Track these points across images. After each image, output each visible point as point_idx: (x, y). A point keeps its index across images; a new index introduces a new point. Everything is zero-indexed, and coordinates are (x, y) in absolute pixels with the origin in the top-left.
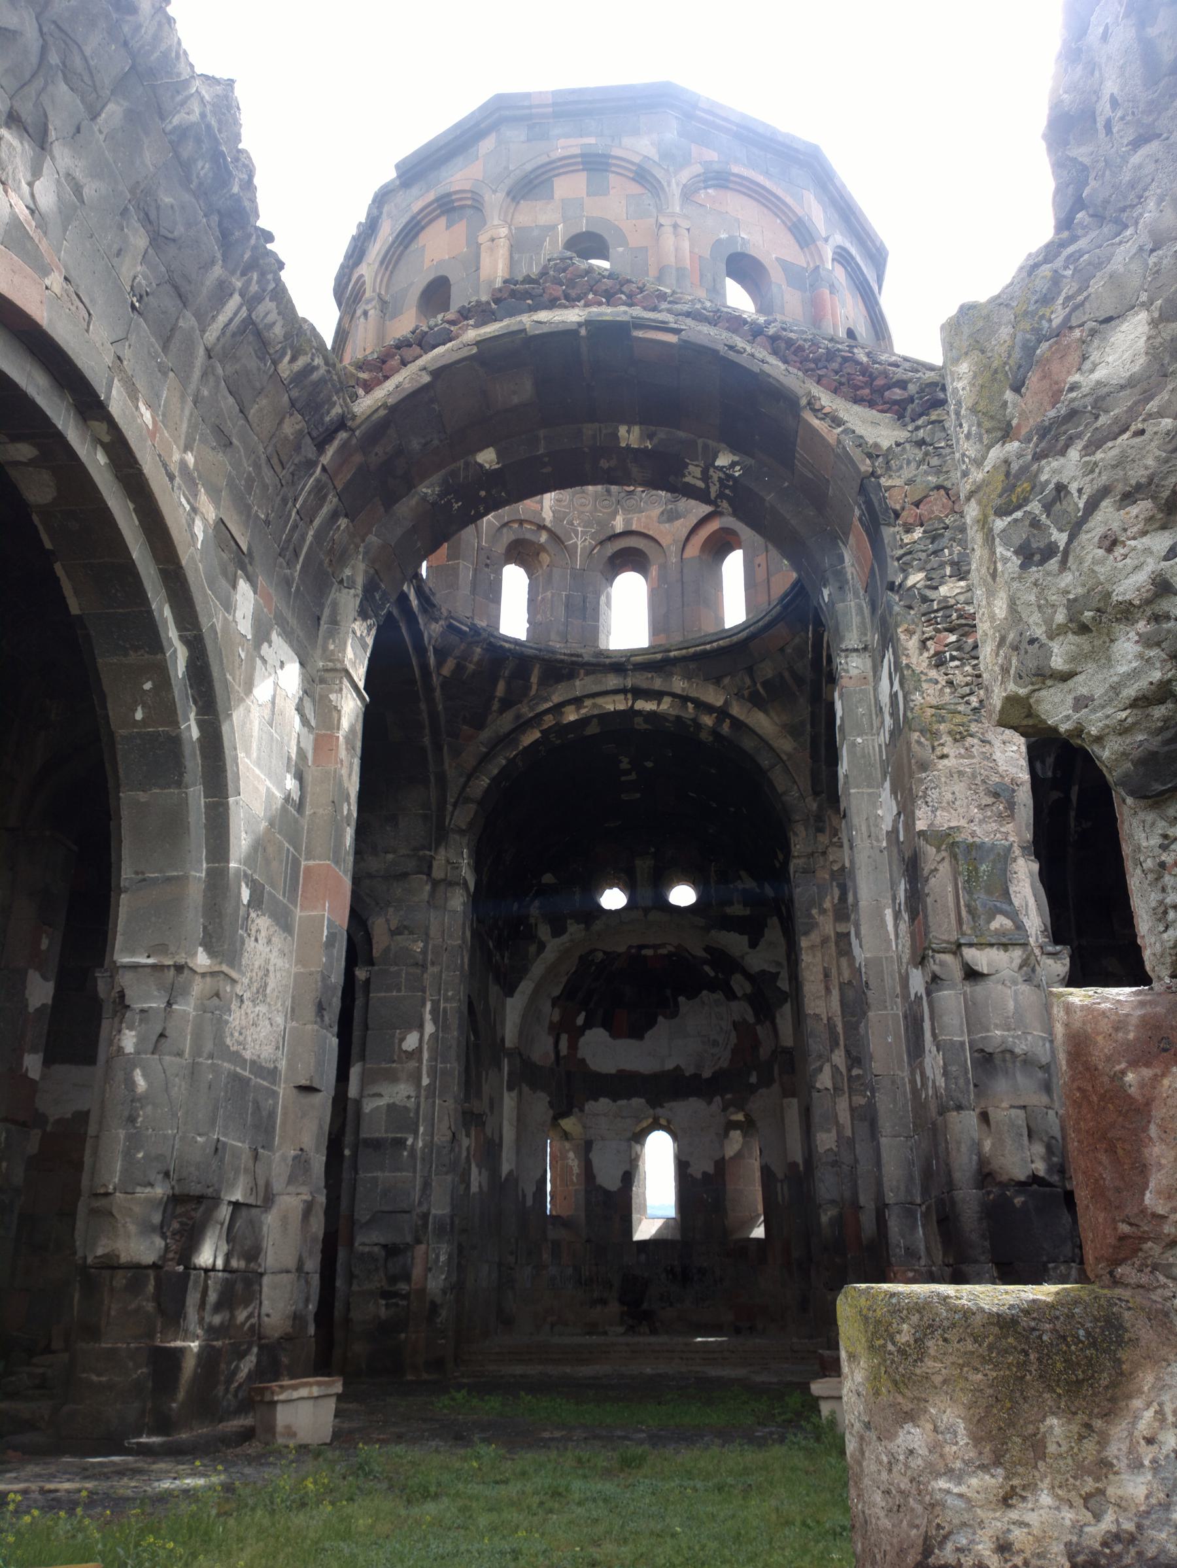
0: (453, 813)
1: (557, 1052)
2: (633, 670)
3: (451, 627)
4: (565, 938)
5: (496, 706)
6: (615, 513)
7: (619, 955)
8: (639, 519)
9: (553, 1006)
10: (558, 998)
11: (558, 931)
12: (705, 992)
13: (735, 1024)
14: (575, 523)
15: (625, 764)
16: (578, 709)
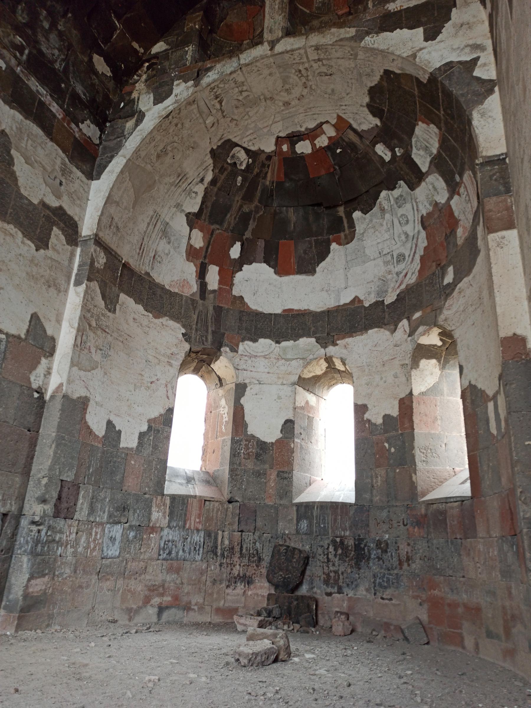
1: (203, 286)
4: (169, 103)
7: (269, 157)
10: (198, 215)
12: (384, 194)
13: (424, 222)
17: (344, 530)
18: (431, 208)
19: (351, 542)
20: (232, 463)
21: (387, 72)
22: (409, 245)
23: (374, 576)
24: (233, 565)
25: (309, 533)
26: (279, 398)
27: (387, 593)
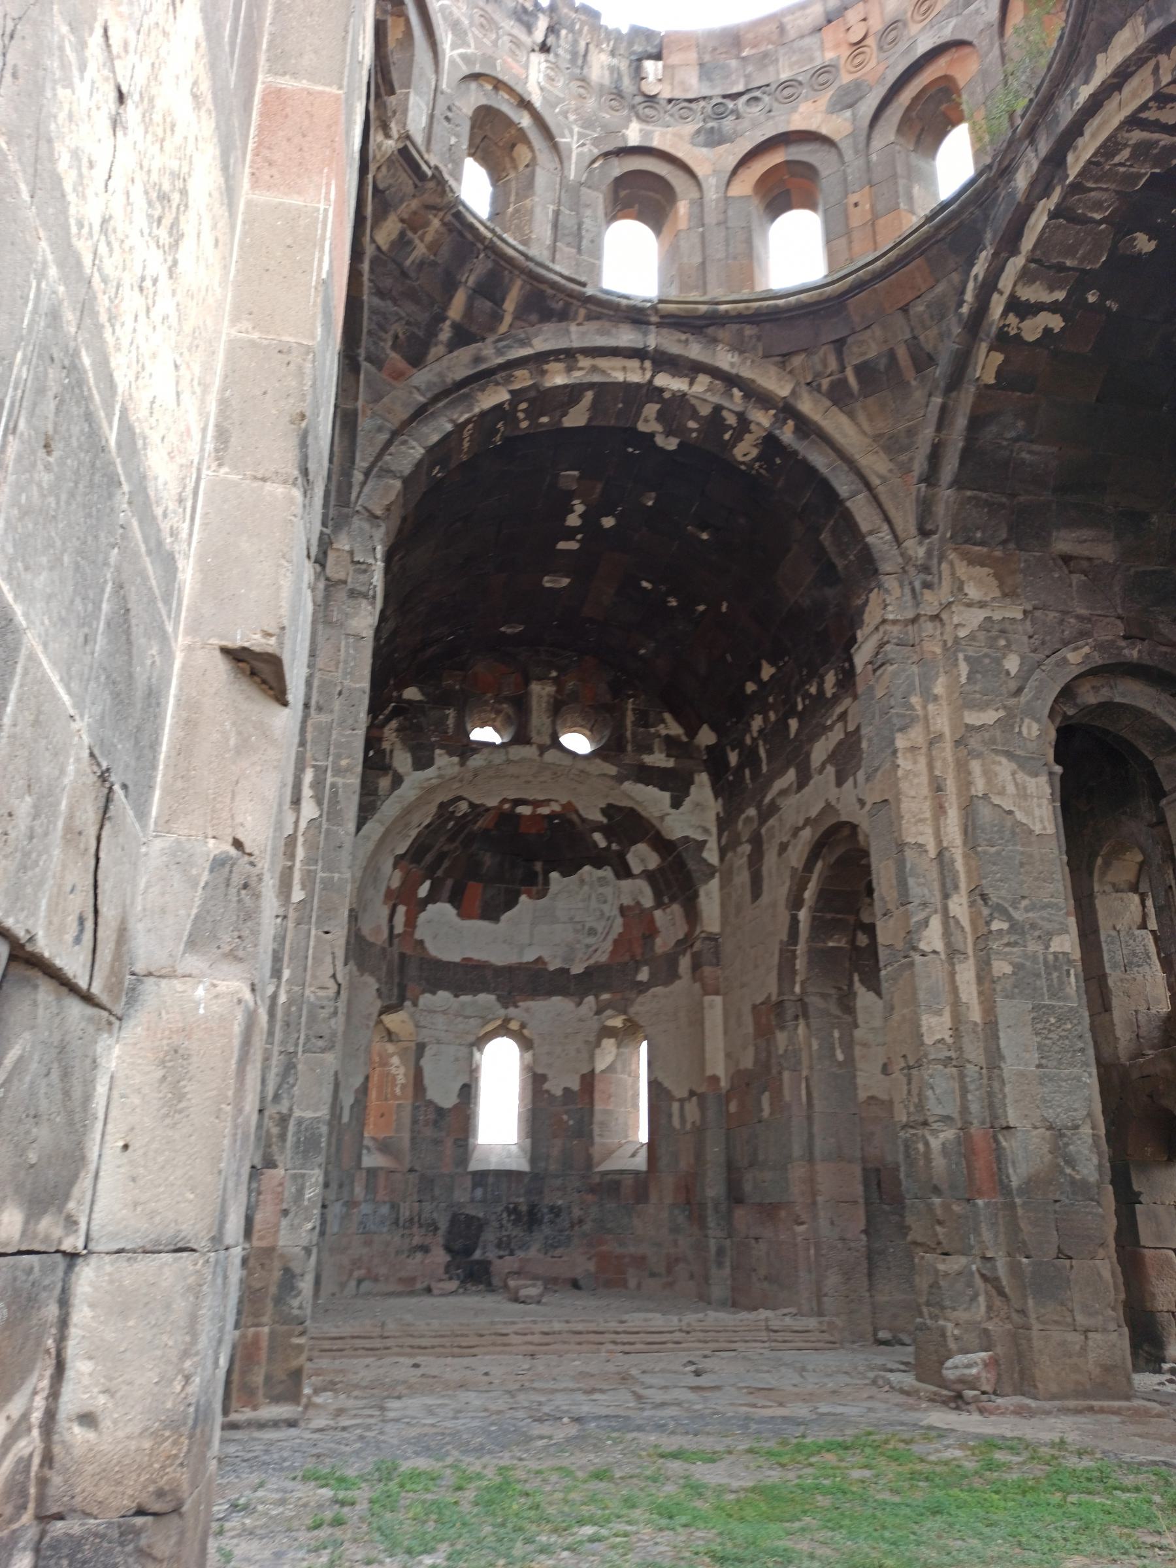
0: (364, 484)
1: (391, 928)
2: (659, 325)
3: (404, 152)
4: (430, 772)
5: (445, 334)
6: (629, 121)
7: (488, 810)
8: (663, 135)
9: (395, 866)
11: (422, 762)
12: (587, 868)
13: (623, 910)
14: (572, 117)
15: (573, 520)
16: (569, 369)
17: (518, 1196)
18: (632, 903)
19: (524, 1209)
20: (412, 1131)
21: (632, 810)
22: (603, 923)
23: (546, 1238)
24: (412, 1235)
25: (483, 1201)
26: (457, 1060)
27: (558, 1252)
